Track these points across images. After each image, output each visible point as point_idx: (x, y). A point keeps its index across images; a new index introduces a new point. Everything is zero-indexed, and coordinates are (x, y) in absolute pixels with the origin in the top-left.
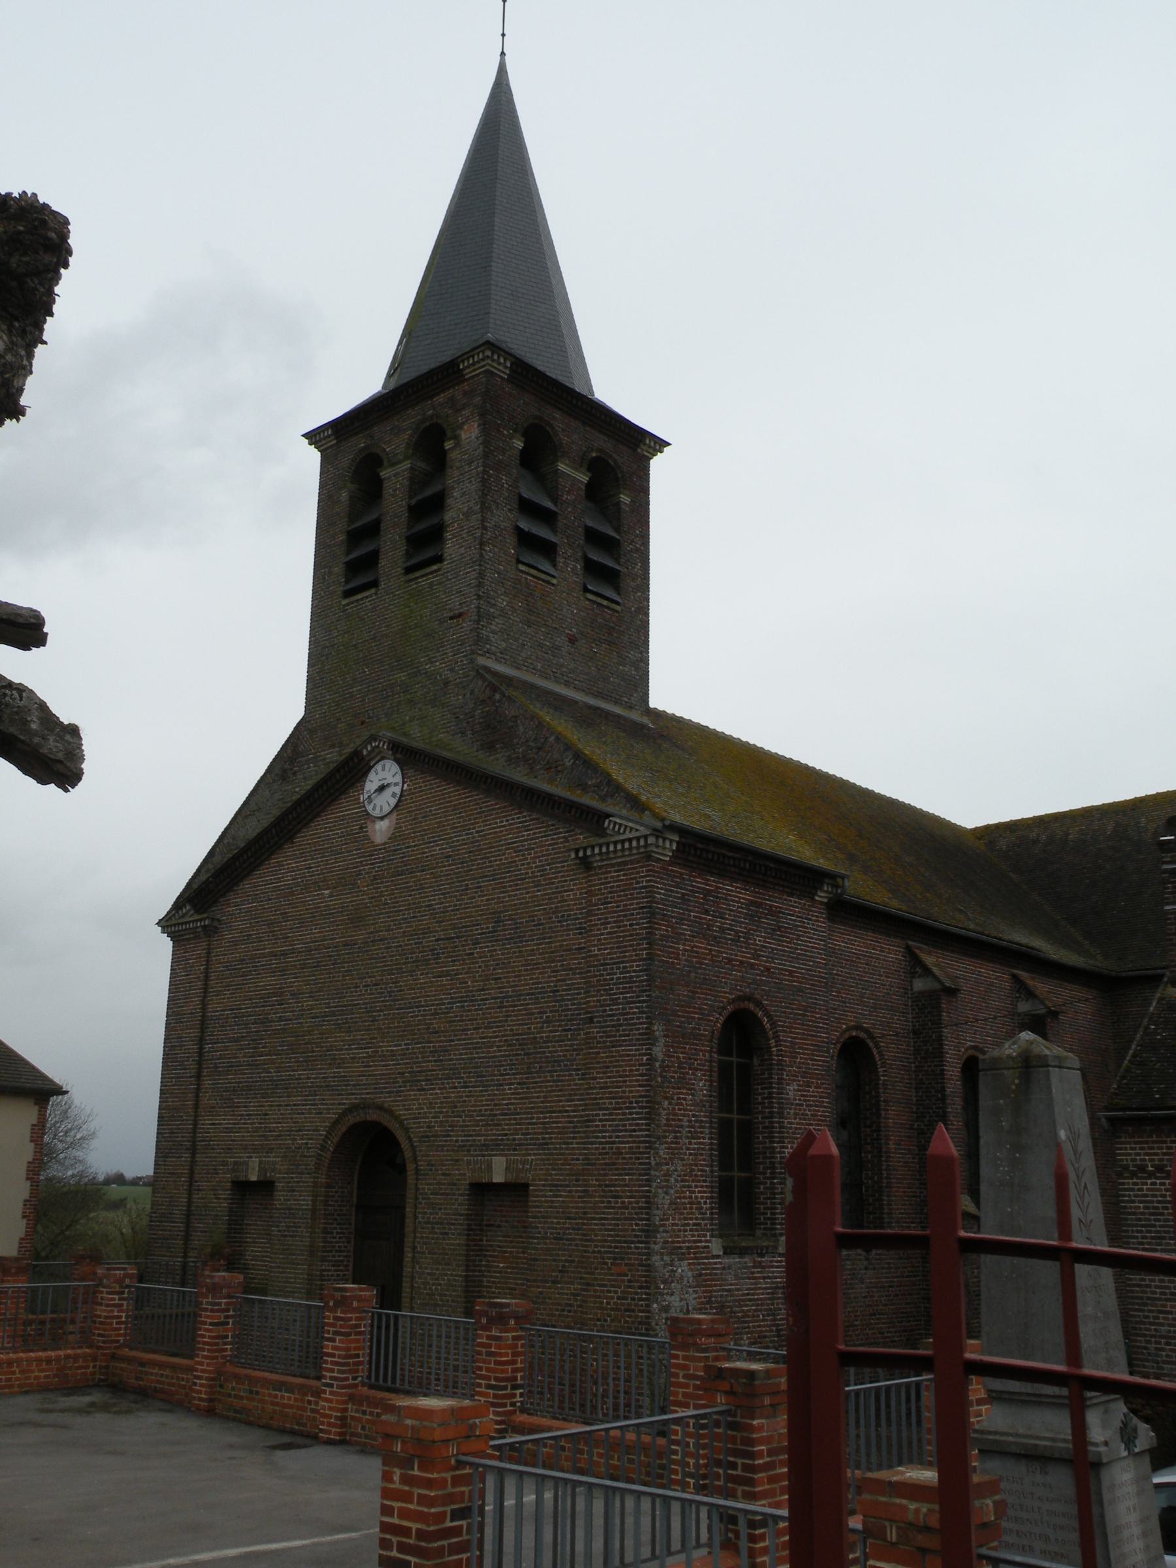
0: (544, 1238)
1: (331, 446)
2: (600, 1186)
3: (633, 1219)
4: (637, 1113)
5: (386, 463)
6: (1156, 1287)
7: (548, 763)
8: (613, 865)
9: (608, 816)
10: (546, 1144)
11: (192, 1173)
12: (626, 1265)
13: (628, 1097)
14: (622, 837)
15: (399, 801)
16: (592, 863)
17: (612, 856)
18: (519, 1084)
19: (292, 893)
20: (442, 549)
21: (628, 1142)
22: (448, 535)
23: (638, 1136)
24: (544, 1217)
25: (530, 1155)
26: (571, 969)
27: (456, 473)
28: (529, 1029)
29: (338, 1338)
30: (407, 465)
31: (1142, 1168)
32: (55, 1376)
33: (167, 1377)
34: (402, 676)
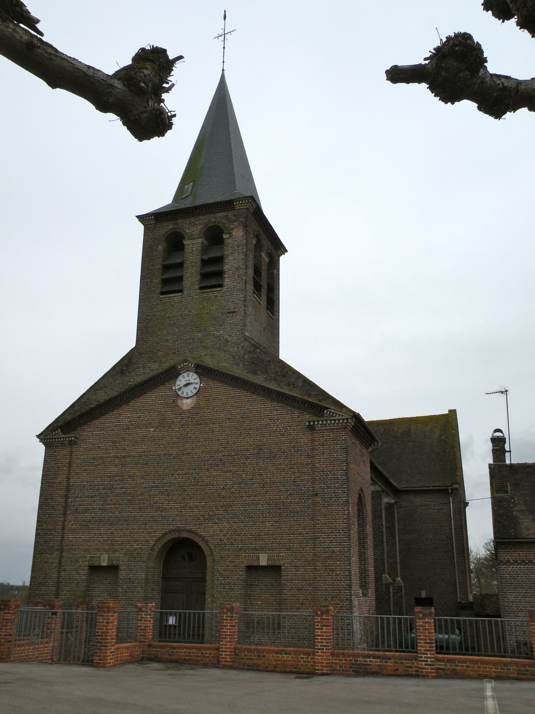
0: (290, 590)
1: (151, 224)
2: (323, 566)
3: (343, 580)
4: (343, 535)
5: (186, 238)
6: (515, 607)
7: (289, 382)
8: (326, 430)
9: (327, 408)
10: (291, 548)
11: (60, 562)
12: (339, 600)
13: (338, 528)
14: (335, 418)
15: (198, 391)
16: (315, 428)
17: (327, 425)
18: (274, 521)
19: (129, 429)
20: (223, 281)
21: (339, 547)
22: (226, 276)
23: (344, 545)
24: (290, 580)
25: (282, 553)
26: (303, 473)
27: (230, 249)
28: (280, 497)
29: (324, 628)
30: (200, 240)
31: (508, 561)
32: (130, 655)
33: (193, 653)
34: (199, 335)
